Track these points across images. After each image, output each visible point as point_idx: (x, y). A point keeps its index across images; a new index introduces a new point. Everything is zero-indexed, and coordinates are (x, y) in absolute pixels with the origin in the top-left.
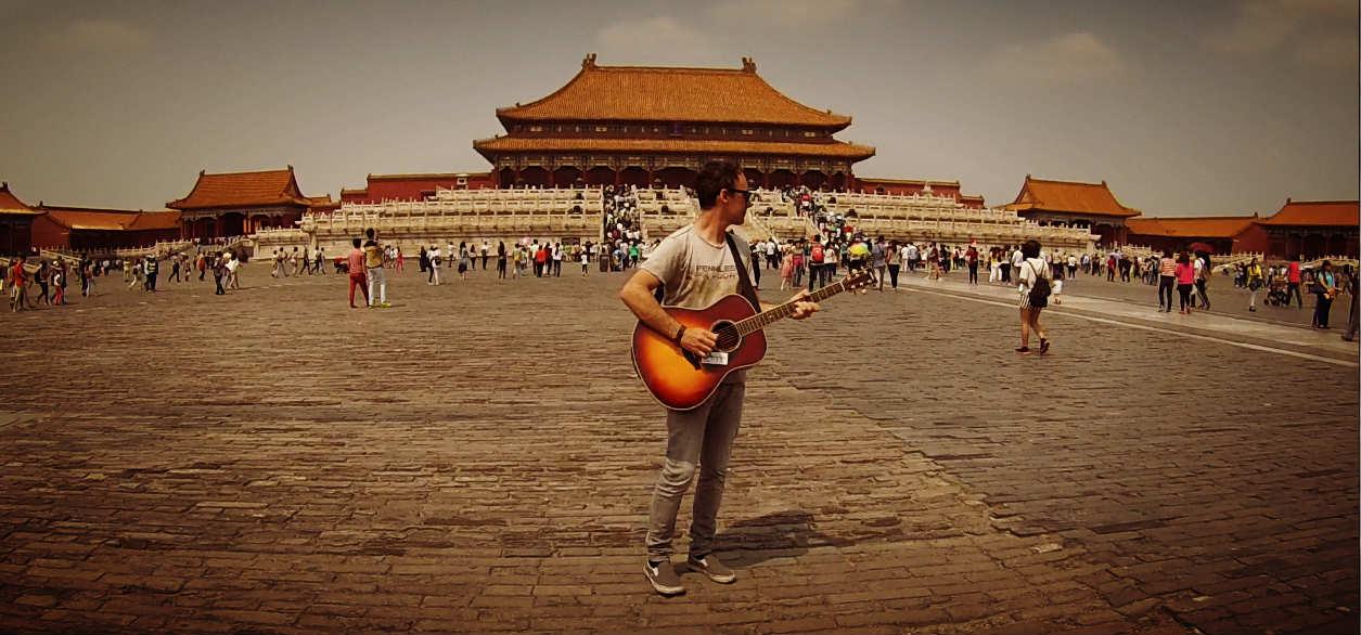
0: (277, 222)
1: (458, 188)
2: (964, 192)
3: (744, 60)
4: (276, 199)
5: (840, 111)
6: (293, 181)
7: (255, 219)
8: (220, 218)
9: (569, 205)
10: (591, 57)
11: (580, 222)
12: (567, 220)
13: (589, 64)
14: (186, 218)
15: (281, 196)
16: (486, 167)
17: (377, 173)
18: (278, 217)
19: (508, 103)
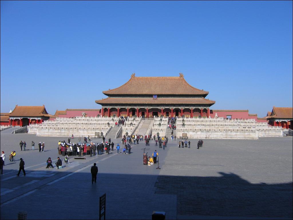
0: (39, 122)
1: (83, 116)
2: (250, 113)
3: (180, 74)
4: (40, 115)
5: (206, 90)
6: (45, 109)
7: (32, 120)
8: (21, 119)
9: (107, 122)
10: (133, 74)
11: (106, 128)
12: (103, 126)
13: (133, 76)
14: (11, 118)
15: (40, 114)
16: (100, 107)
17: (68, 109)
18: (39, 120)
19: (106, 90)
